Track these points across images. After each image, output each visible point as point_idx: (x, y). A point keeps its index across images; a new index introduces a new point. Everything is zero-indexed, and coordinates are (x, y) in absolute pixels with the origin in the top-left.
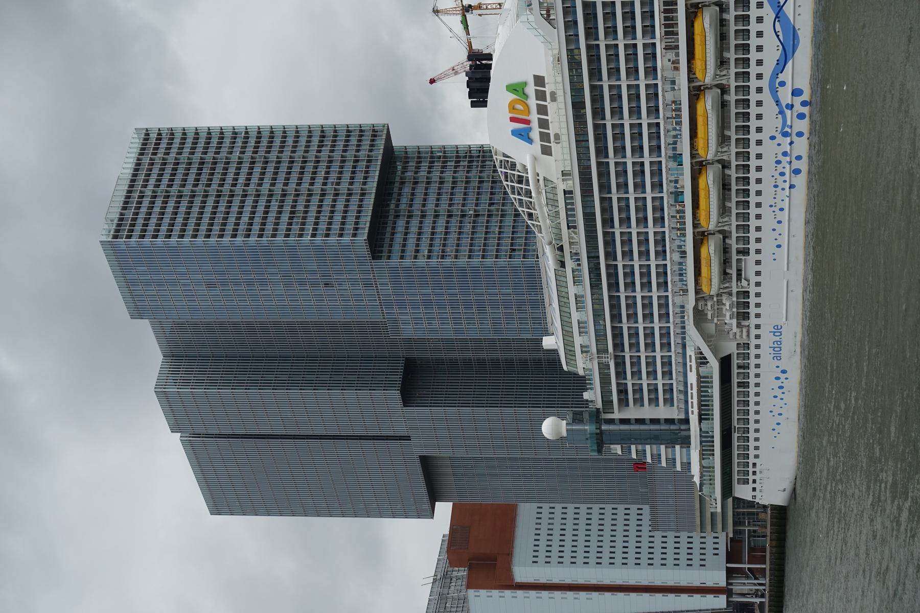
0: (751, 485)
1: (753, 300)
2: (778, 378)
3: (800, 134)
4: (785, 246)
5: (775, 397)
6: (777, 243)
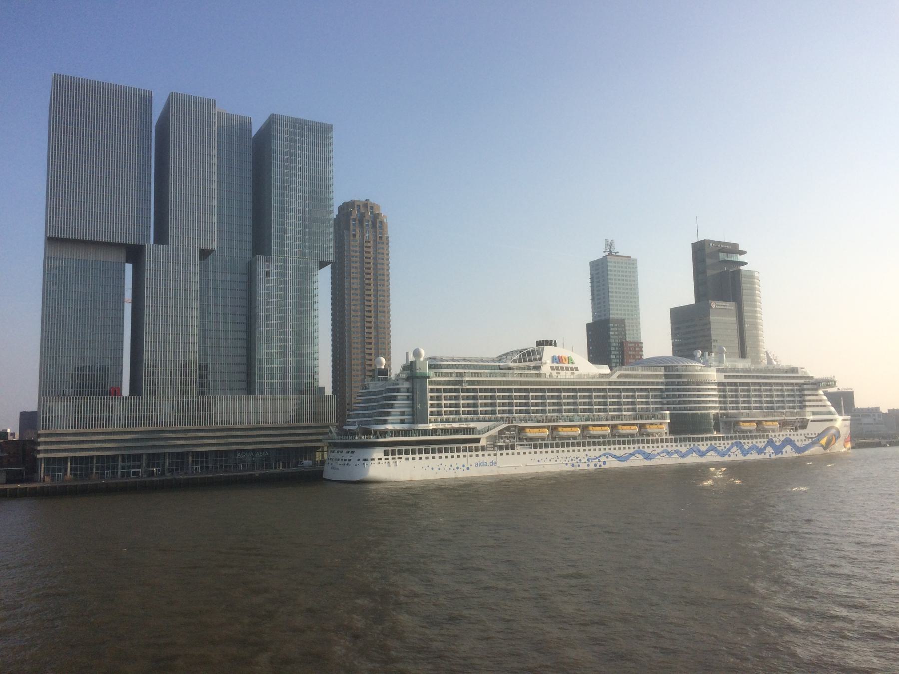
0: (383, 457)
1: (510, 452)
2: (464, 466)
3: (588, 465)
4: (557, 463)
5: (451, 466)
6: (540, 460)
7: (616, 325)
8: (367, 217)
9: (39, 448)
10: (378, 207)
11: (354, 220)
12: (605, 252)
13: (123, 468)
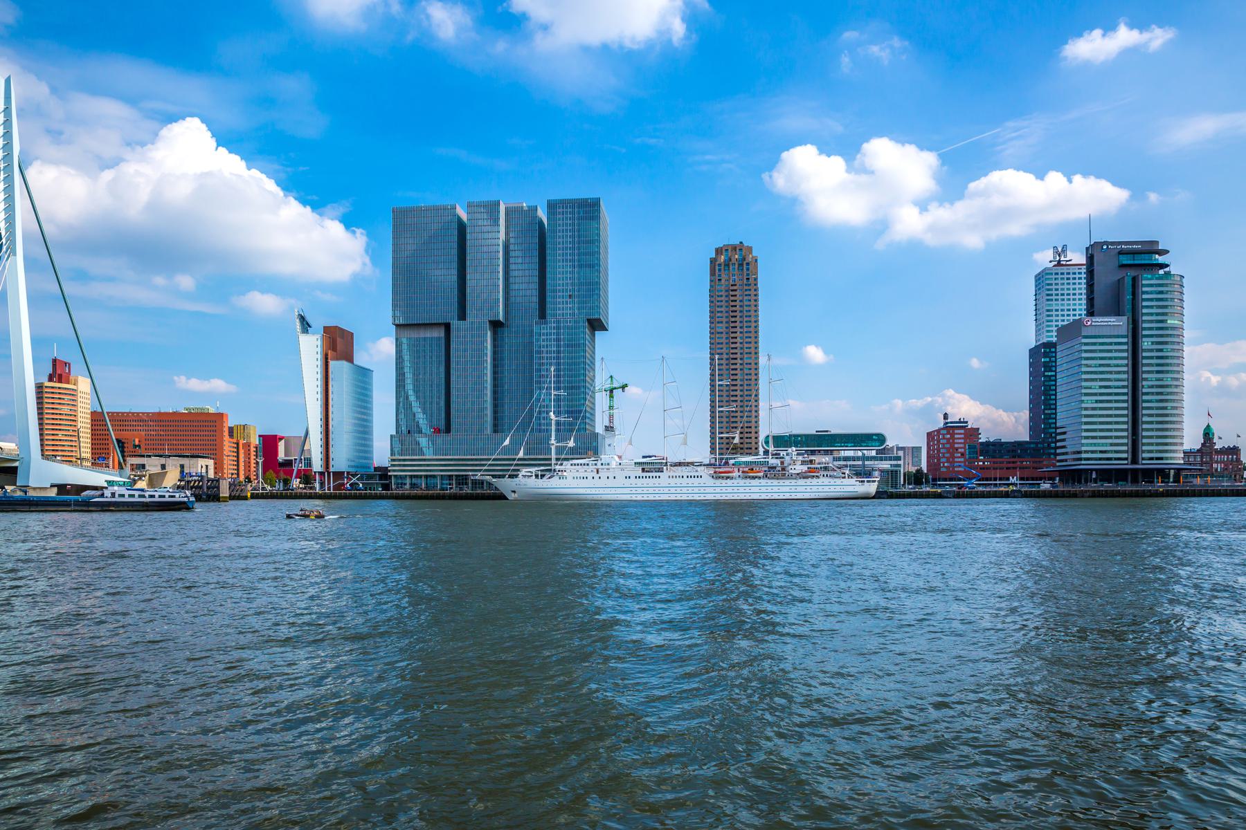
8: (733, 261)
10: (750, 249)
11: (720, 265)
12: (1051, 262)
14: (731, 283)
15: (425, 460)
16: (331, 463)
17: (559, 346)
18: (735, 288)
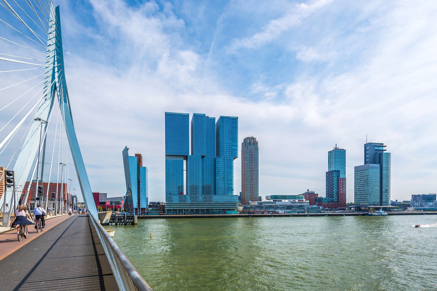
7: (336, 172)
9: (165, 207)
11: (248, 143)
13: (184, 212)
14: (251, 149)
15: (186, 204)
16: (141, 205)
17: (225, 166)
18: (252, 150)
